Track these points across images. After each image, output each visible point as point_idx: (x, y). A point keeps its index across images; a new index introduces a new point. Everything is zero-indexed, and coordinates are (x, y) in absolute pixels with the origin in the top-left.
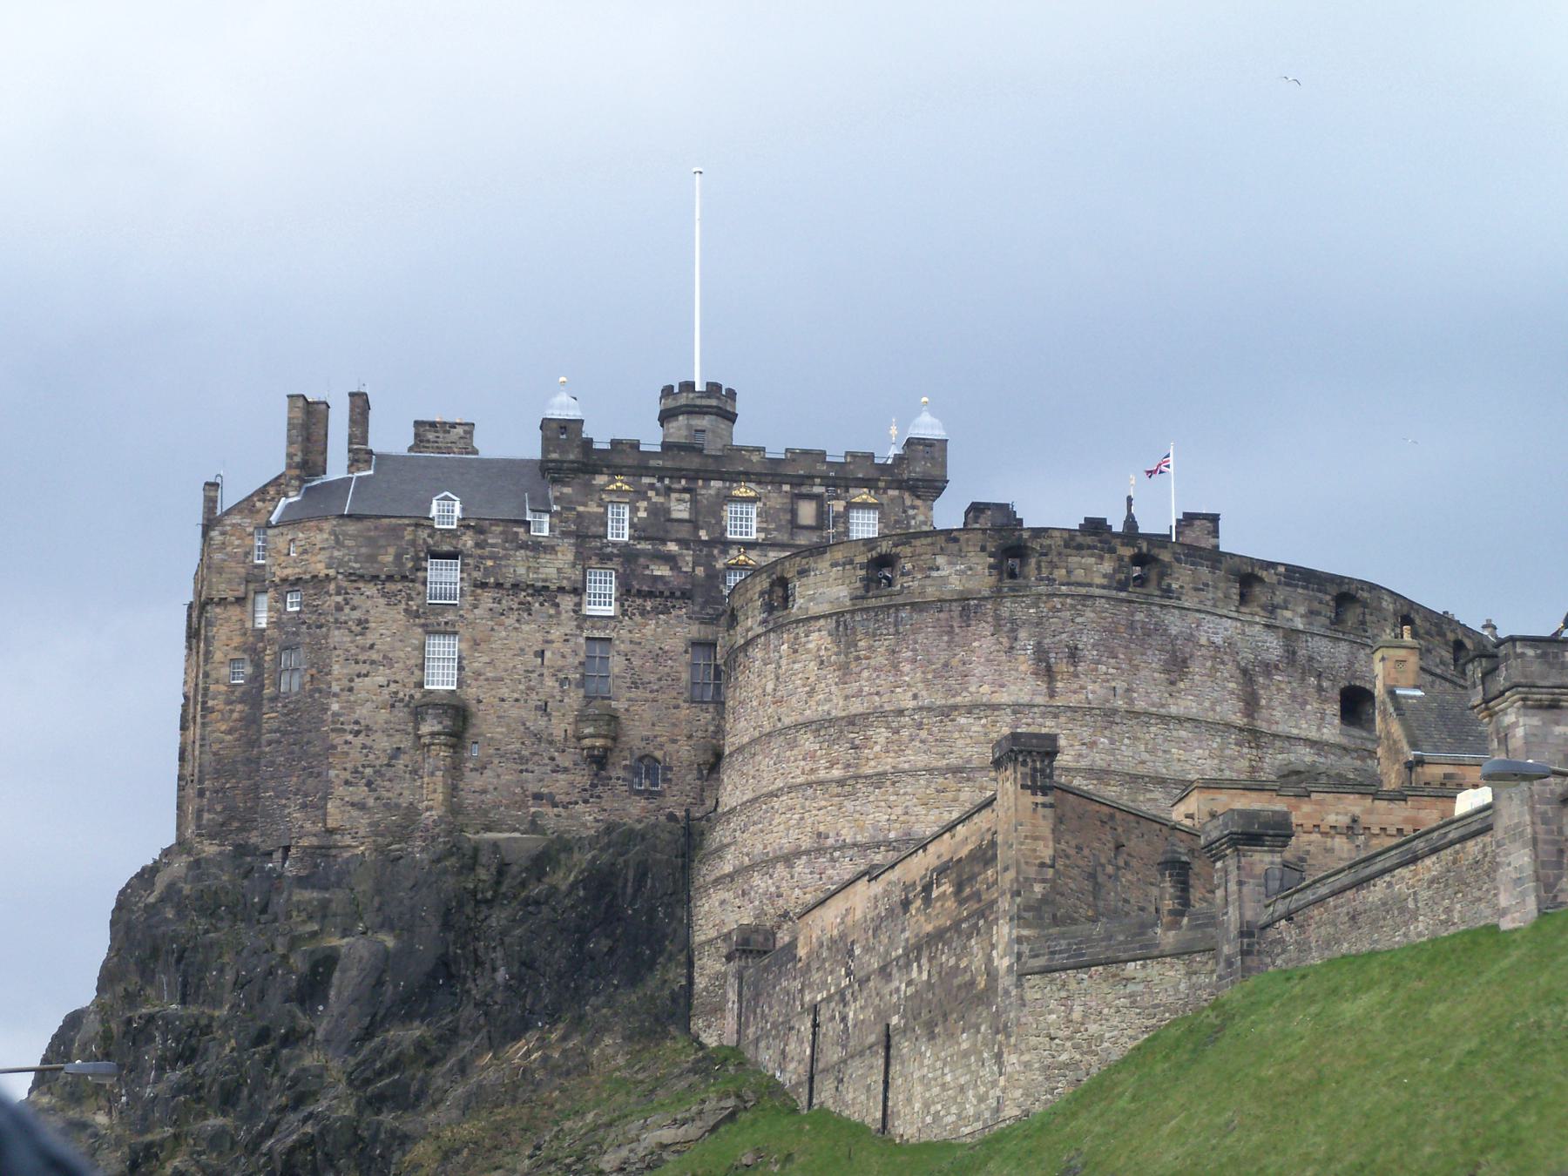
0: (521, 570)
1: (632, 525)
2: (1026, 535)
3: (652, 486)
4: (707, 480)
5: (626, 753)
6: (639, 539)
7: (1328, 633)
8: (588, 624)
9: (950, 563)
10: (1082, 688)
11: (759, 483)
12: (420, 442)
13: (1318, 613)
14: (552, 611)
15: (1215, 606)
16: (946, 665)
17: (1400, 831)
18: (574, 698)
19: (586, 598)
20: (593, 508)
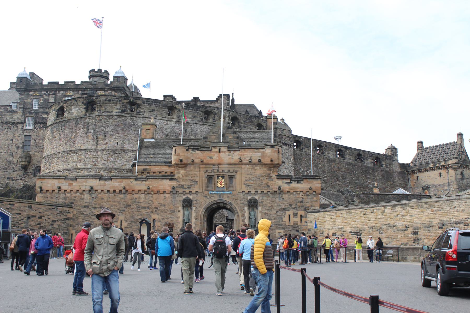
0: (8, 118)
1: (39, 105)
2: (94, 98)
3: (45, 94)
4: (59, 91)
5: (33, 166)
6: (40, 108)
7: (200, 123)
8: (25, 132)
9: (75, 108)
10: (107, 143)
11: (73, 91)
12: (11, 88)
13: (197, 117)
14: (16, 129)
15: (157, 116)
16: (71, 138)
17: (108, 191)
18: (20, 152)
19: (25, 124)
20: (29, 101)
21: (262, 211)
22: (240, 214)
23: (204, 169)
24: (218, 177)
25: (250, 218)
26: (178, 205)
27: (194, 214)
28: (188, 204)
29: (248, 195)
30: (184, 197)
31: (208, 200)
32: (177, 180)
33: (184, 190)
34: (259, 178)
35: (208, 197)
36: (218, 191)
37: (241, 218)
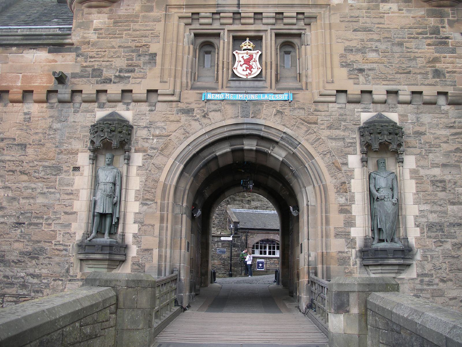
21: (422, 172)
22: (329, 181)
23: (187, 12)
24: (238, 40)
25: (372, 199)
26: (77, 145)
27: (135, 183)
28: (112, 140)
29: (357, 108)
30: (101, 114)
31: (195, 125)
32: (78, 49)
33: (101, 87)
34: (401, 44)
35: (197, 113)
36: (237, 91)
37: (336, 200)
